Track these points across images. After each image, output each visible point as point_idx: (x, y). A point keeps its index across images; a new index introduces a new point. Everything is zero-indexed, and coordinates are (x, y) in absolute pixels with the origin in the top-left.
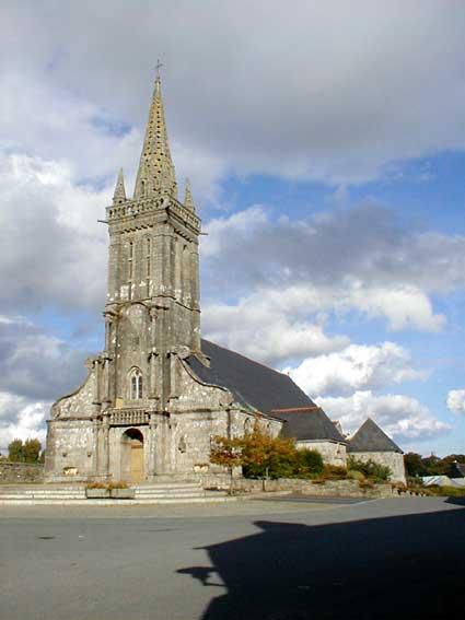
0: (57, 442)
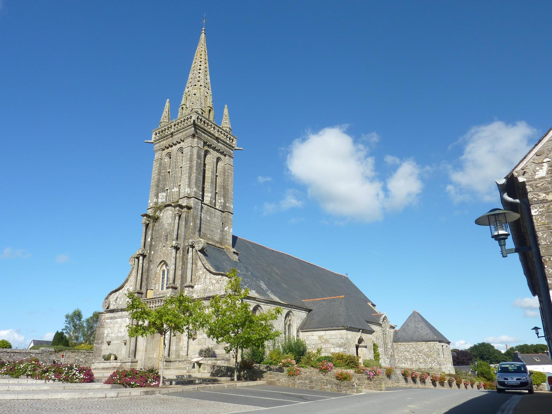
0: (106, 331)
